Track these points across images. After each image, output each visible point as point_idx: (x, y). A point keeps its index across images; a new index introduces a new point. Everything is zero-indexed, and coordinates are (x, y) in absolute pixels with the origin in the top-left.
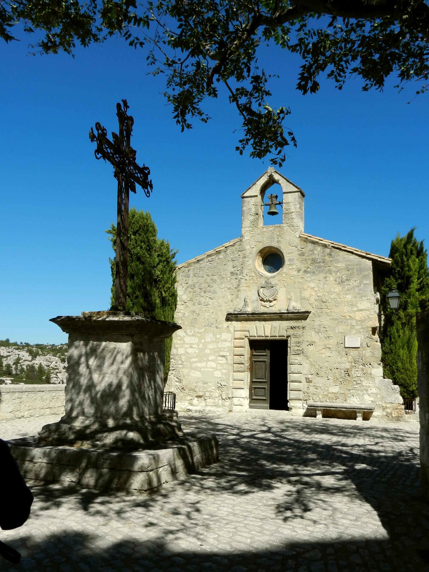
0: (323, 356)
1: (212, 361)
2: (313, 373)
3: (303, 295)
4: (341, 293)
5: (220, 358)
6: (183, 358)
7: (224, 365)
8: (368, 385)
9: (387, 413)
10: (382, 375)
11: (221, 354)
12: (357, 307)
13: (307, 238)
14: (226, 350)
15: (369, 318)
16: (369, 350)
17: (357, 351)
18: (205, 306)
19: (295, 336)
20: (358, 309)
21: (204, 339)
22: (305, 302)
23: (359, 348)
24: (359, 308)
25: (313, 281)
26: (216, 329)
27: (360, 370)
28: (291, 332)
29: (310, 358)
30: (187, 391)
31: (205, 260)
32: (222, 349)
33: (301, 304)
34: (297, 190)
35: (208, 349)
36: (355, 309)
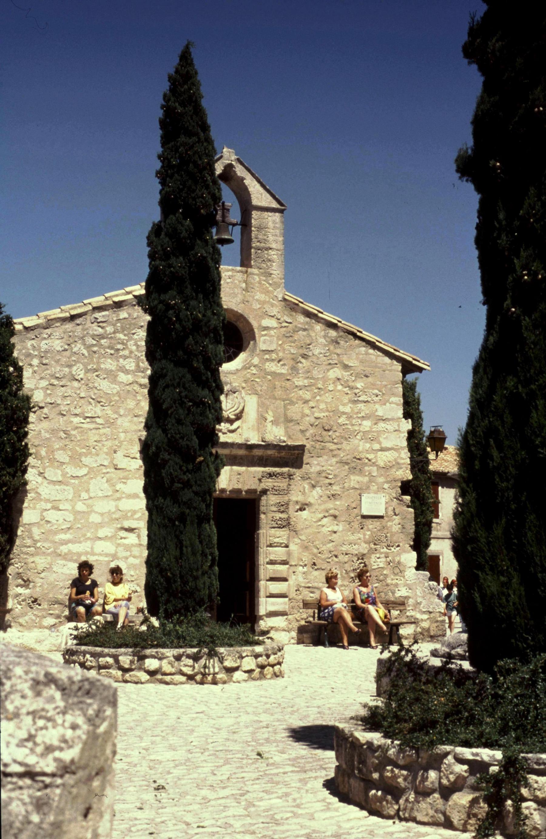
0: (325, 530)
1: (106, 538)
2: (306, 562)
3: (290, 414)
4: (355, 416)
5: (123, 534)
6: (36, 531)
7: (133, 549)
8: (394, 582)
9: (423, 629)
10: (415, 564)
11: (126, 524)
12: (380, 443)
13: (297, 305)
14: (136, 516)
15: (398, 463)
16: (397, 519)
17: (378, 523)
18: (88, 420)
19: (278, 492)
20: (382, 448)
21: (88, 491)
22: (293, 427)
23: (381, 517)
24: (383, 446)
25: (309, 388)
26: (113, 470)
27: (383, 555)
28: (268, 483)
29: (301, 535)
30: (45, 605)
31: (88, 317)
32: (129, 514)
33: (287, 432)
34: (275, 205)
35: (96, 512)
36: (376, 446)
